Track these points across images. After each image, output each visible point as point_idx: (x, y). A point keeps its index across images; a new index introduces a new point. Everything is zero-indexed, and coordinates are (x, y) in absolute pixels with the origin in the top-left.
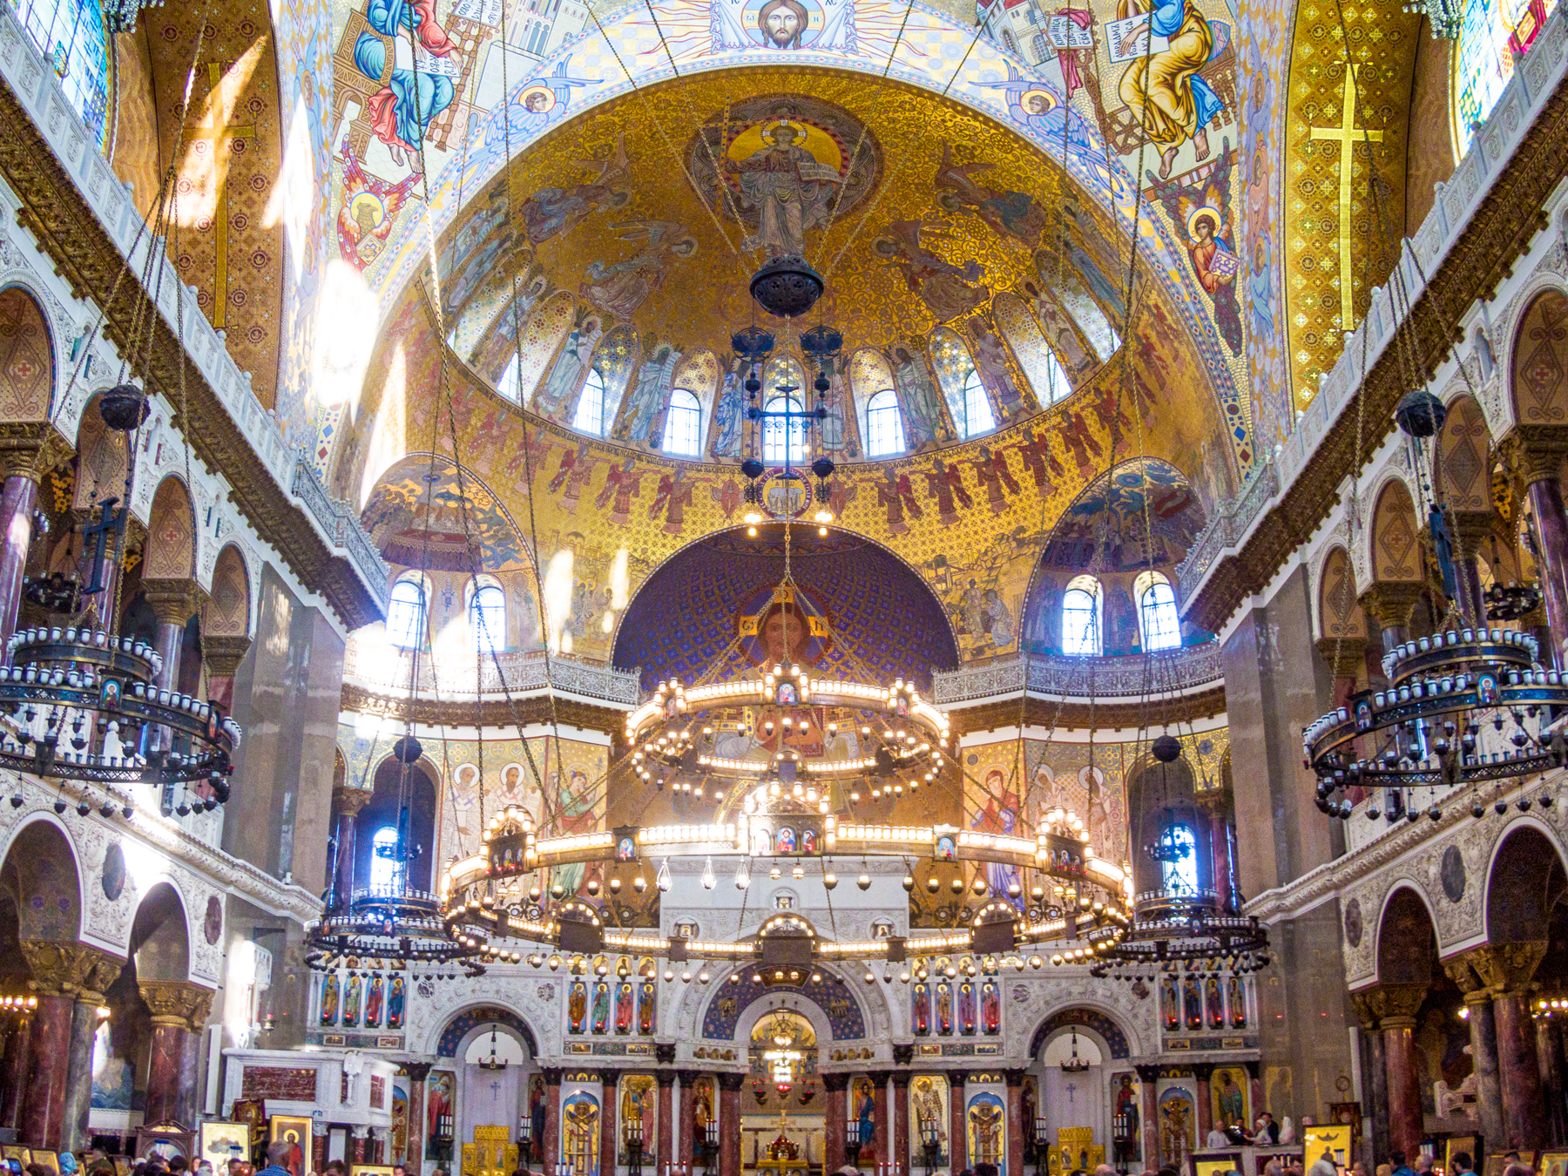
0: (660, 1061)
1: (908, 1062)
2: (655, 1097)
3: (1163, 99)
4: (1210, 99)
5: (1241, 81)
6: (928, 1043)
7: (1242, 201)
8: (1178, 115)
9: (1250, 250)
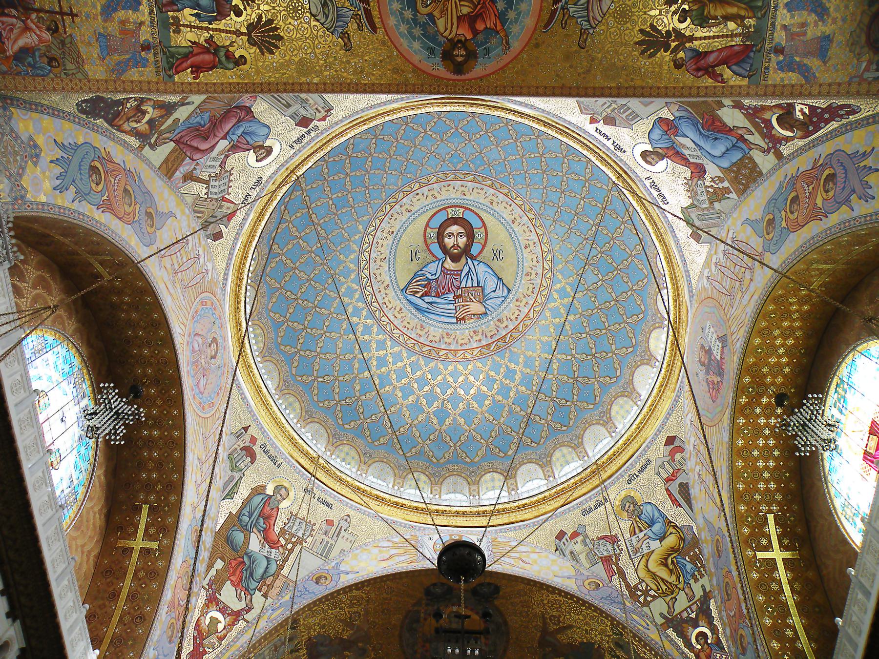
3: (663, 573)
4: (689, 566)
5: (705, 551)
7: (721, 618)
8: (672, 579)
9: (735, 642)
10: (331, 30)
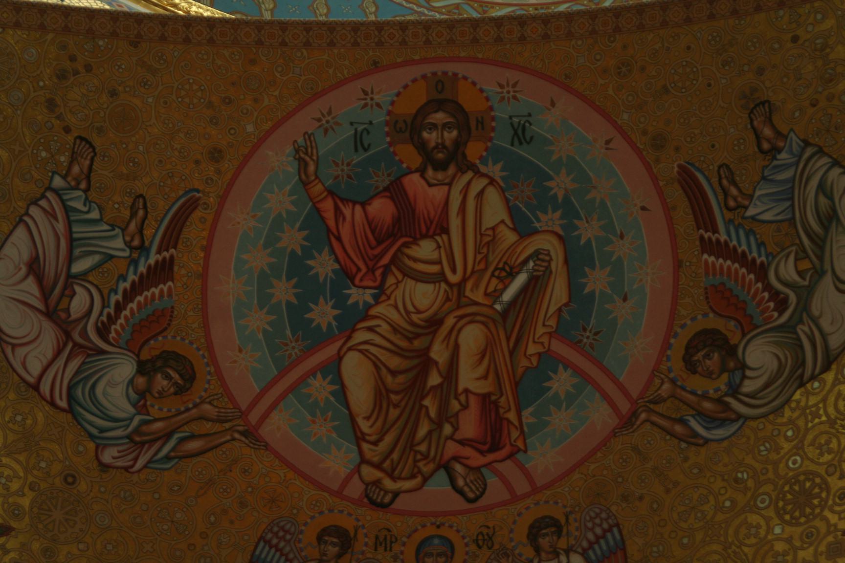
10: (809, 151)
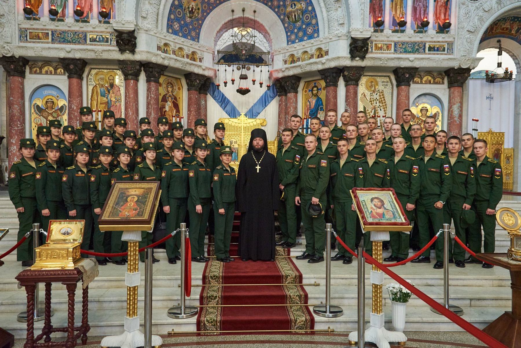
0: (122, 51)
1: (363, 58)
2: (123, 91)
6: (380, 38)
